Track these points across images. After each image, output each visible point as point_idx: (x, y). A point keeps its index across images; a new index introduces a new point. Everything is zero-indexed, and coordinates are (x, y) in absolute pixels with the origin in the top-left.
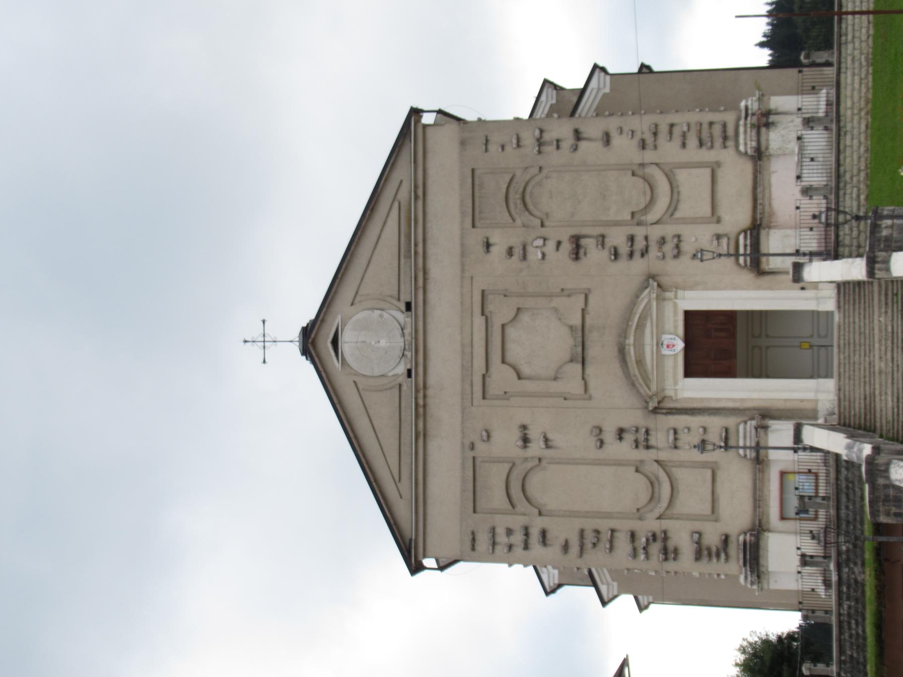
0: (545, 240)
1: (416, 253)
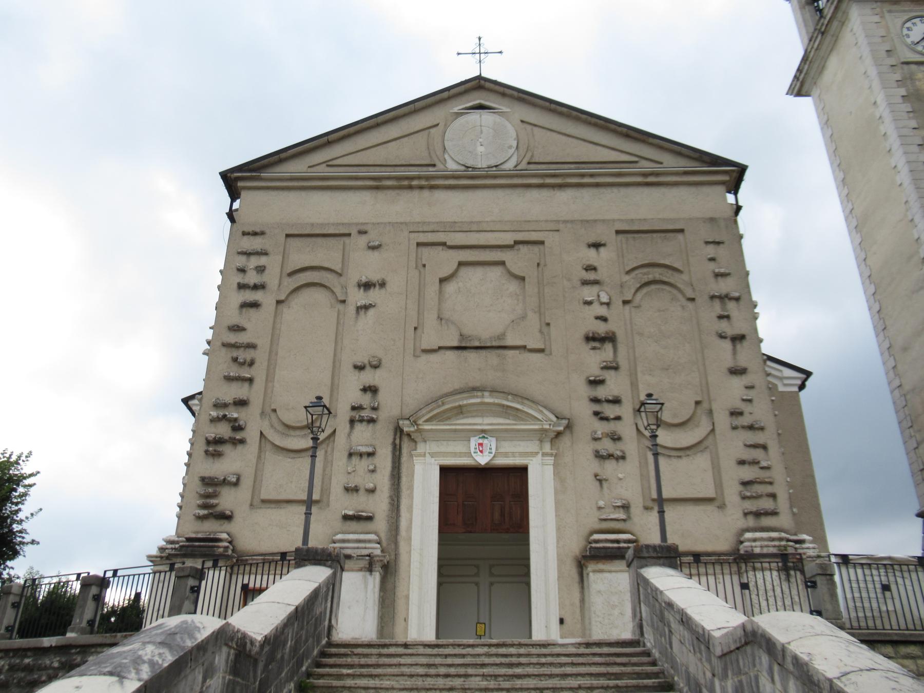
0: (608, 304)
1: (583, 175)
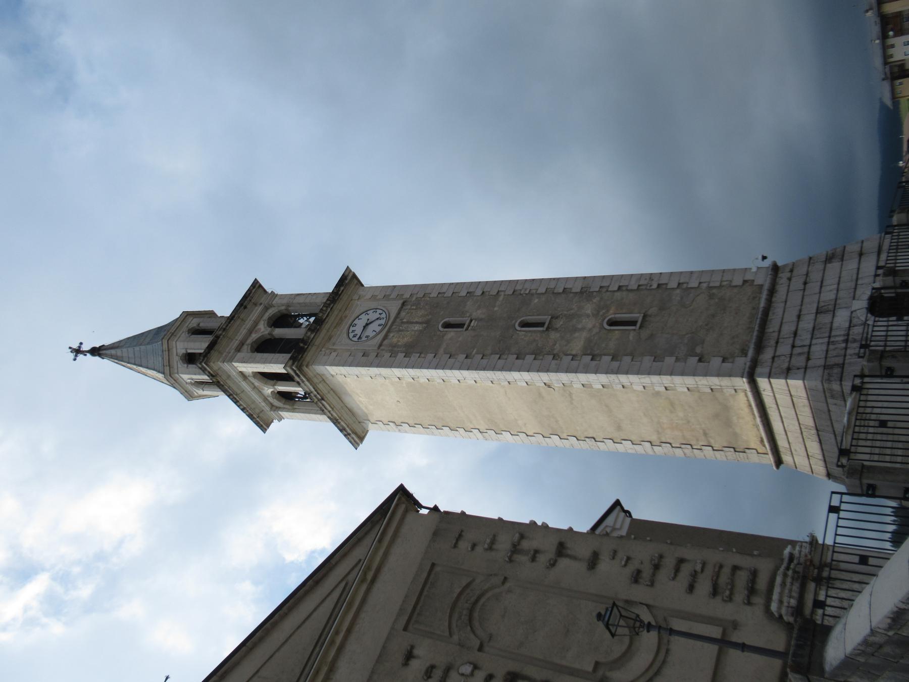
0: (476, 667)
